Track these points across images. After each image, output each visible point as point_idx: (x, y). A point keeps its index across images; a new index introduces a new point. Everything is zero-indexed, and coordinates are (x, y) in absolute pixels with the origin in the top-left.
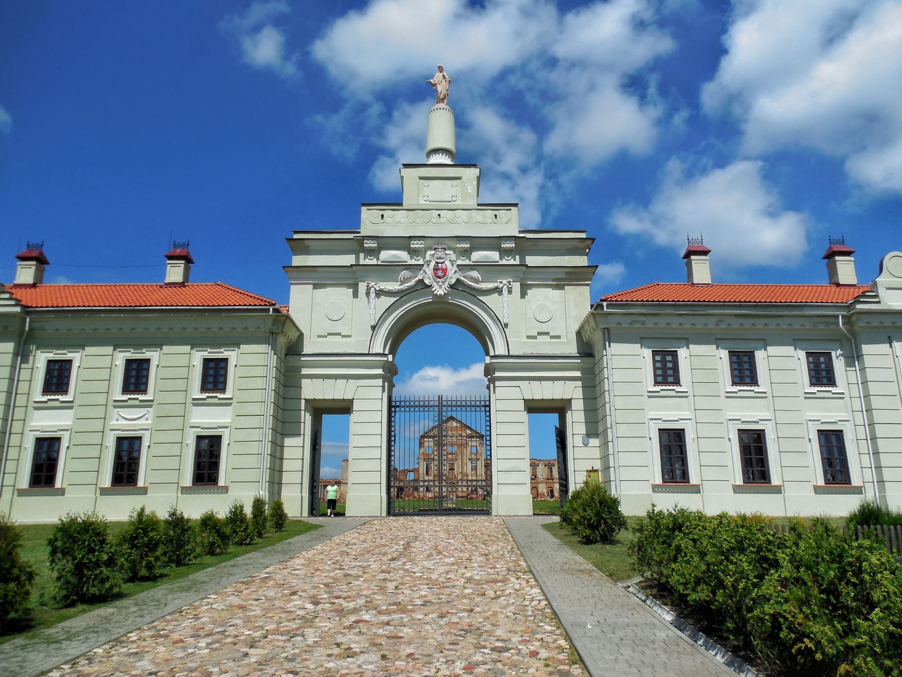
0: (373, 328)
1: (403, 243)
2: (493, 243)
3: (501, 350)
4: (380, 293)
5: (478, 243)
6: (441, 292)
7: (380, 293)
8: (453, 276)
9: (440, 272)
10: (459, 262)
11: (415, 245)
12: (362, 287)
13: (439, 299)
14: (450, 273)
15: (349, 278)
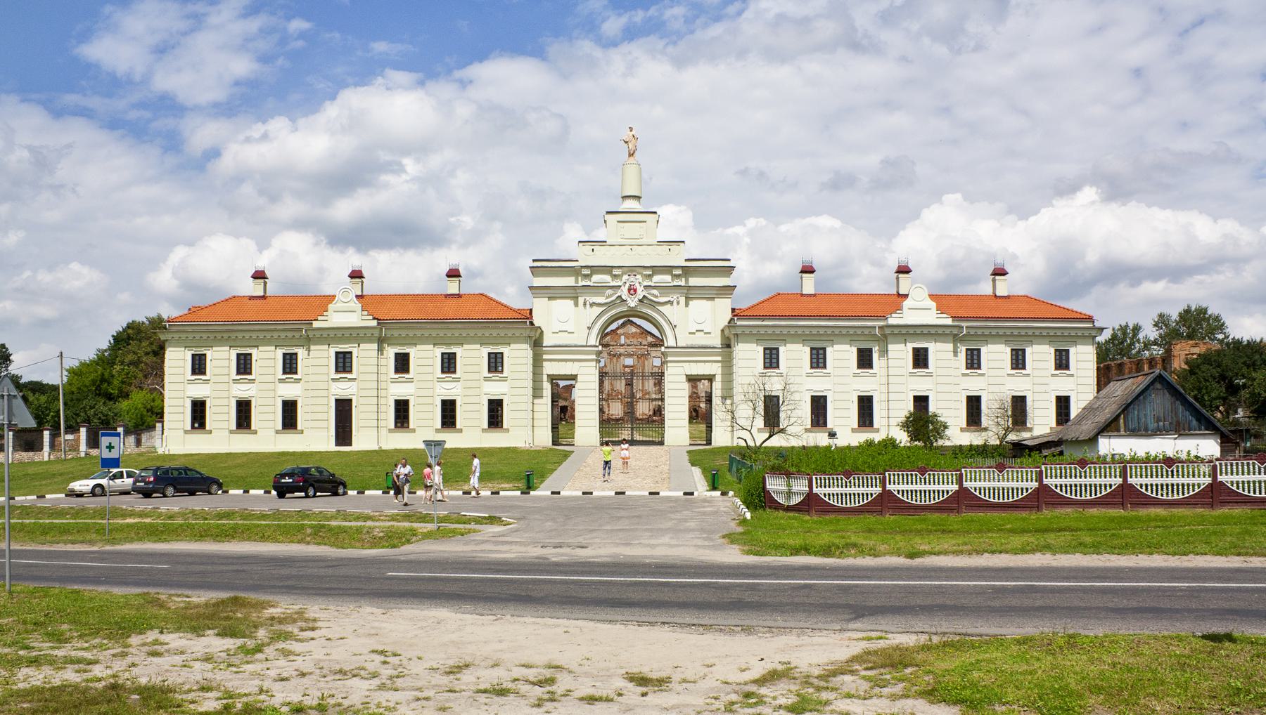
0: (589, 328)
1: (607, 270)
2: (667, 269)
3: (671, 342)
4: (593, 304)
5: (656, 270)
6: (632, 305)
7: (593, 304)
8: (641, 293)
9: (633, 291)
10: (645, 284)
11: (616, 272)
12: (581, 300)
13: (632, 309)
14: (639, 291)
15: (573, 293)
